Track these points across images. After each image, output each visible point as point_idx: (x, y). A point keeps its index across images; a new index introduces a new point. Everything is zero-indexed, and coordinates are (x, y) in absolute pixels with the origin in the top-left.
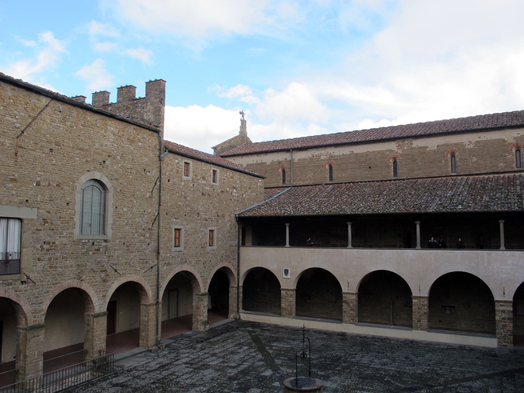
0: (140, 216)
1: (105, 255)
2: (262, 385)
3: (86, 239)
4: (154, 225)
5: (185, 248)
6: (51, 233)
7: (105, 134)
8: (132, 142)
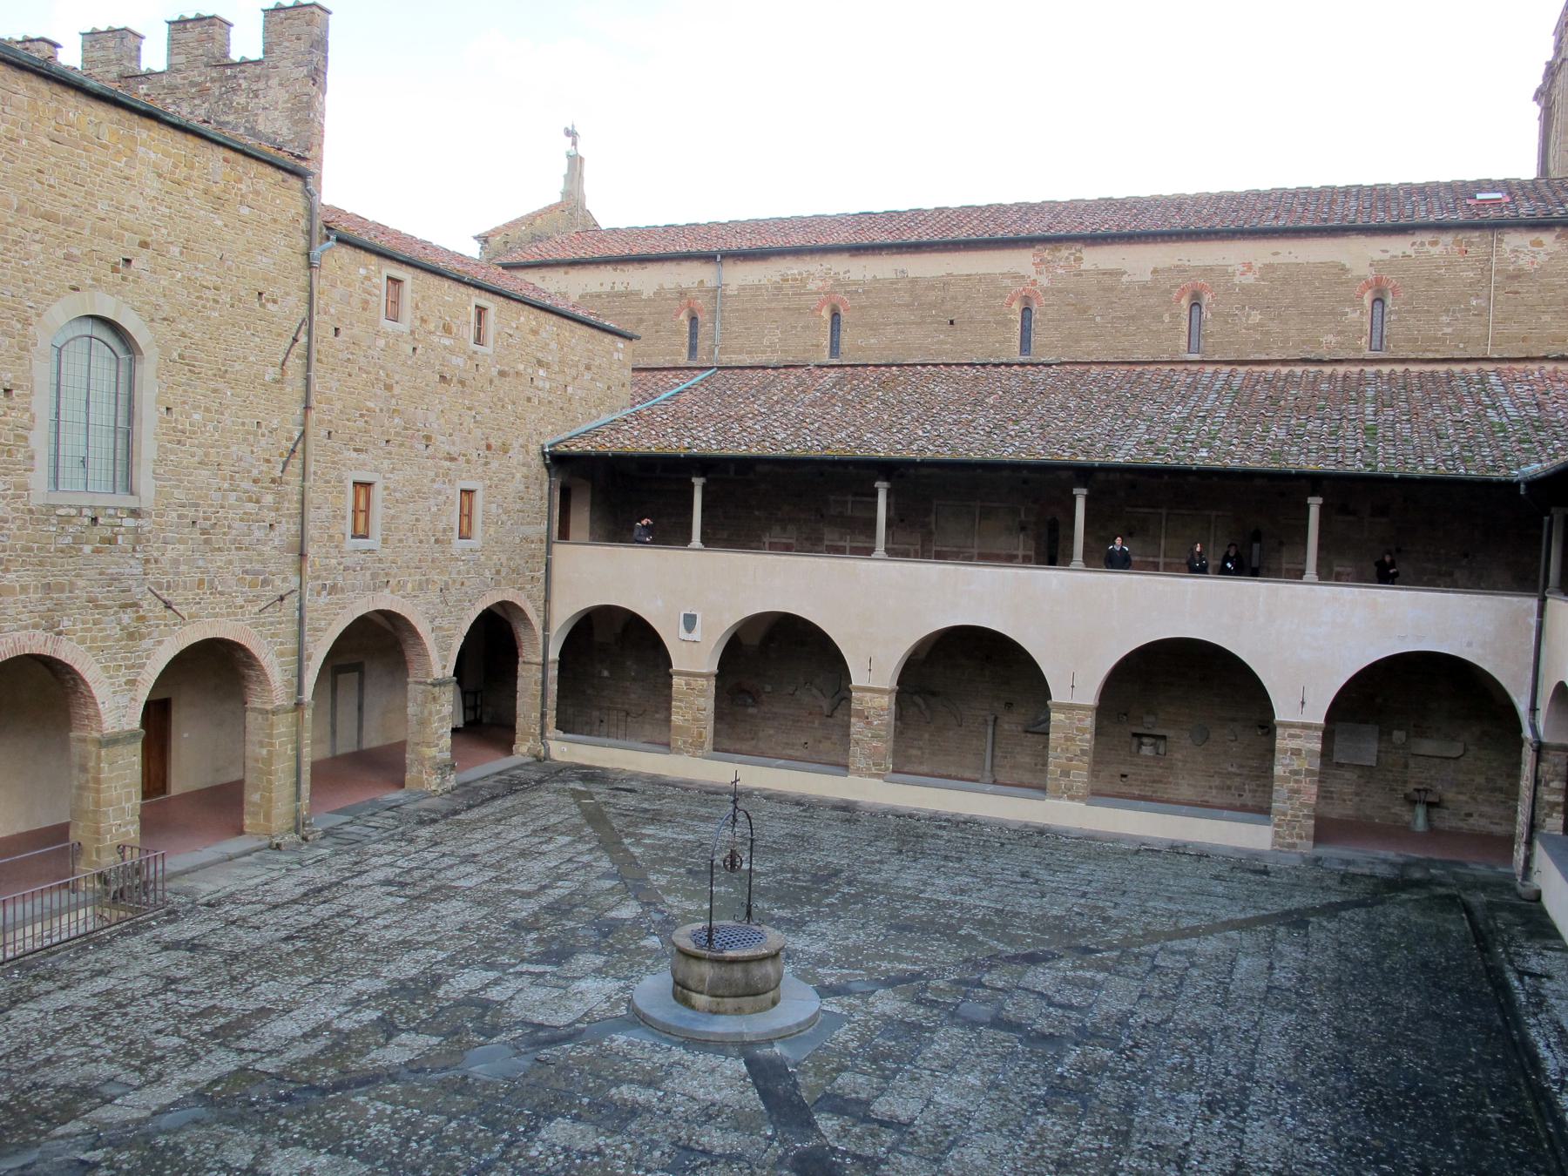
0: (245, 440)
1: (133, 557)
2: (611, 946)
3: (70, 506)
4: (289, 468)
5: (385, 541)
7: (127, 172)
8: (218, 203)
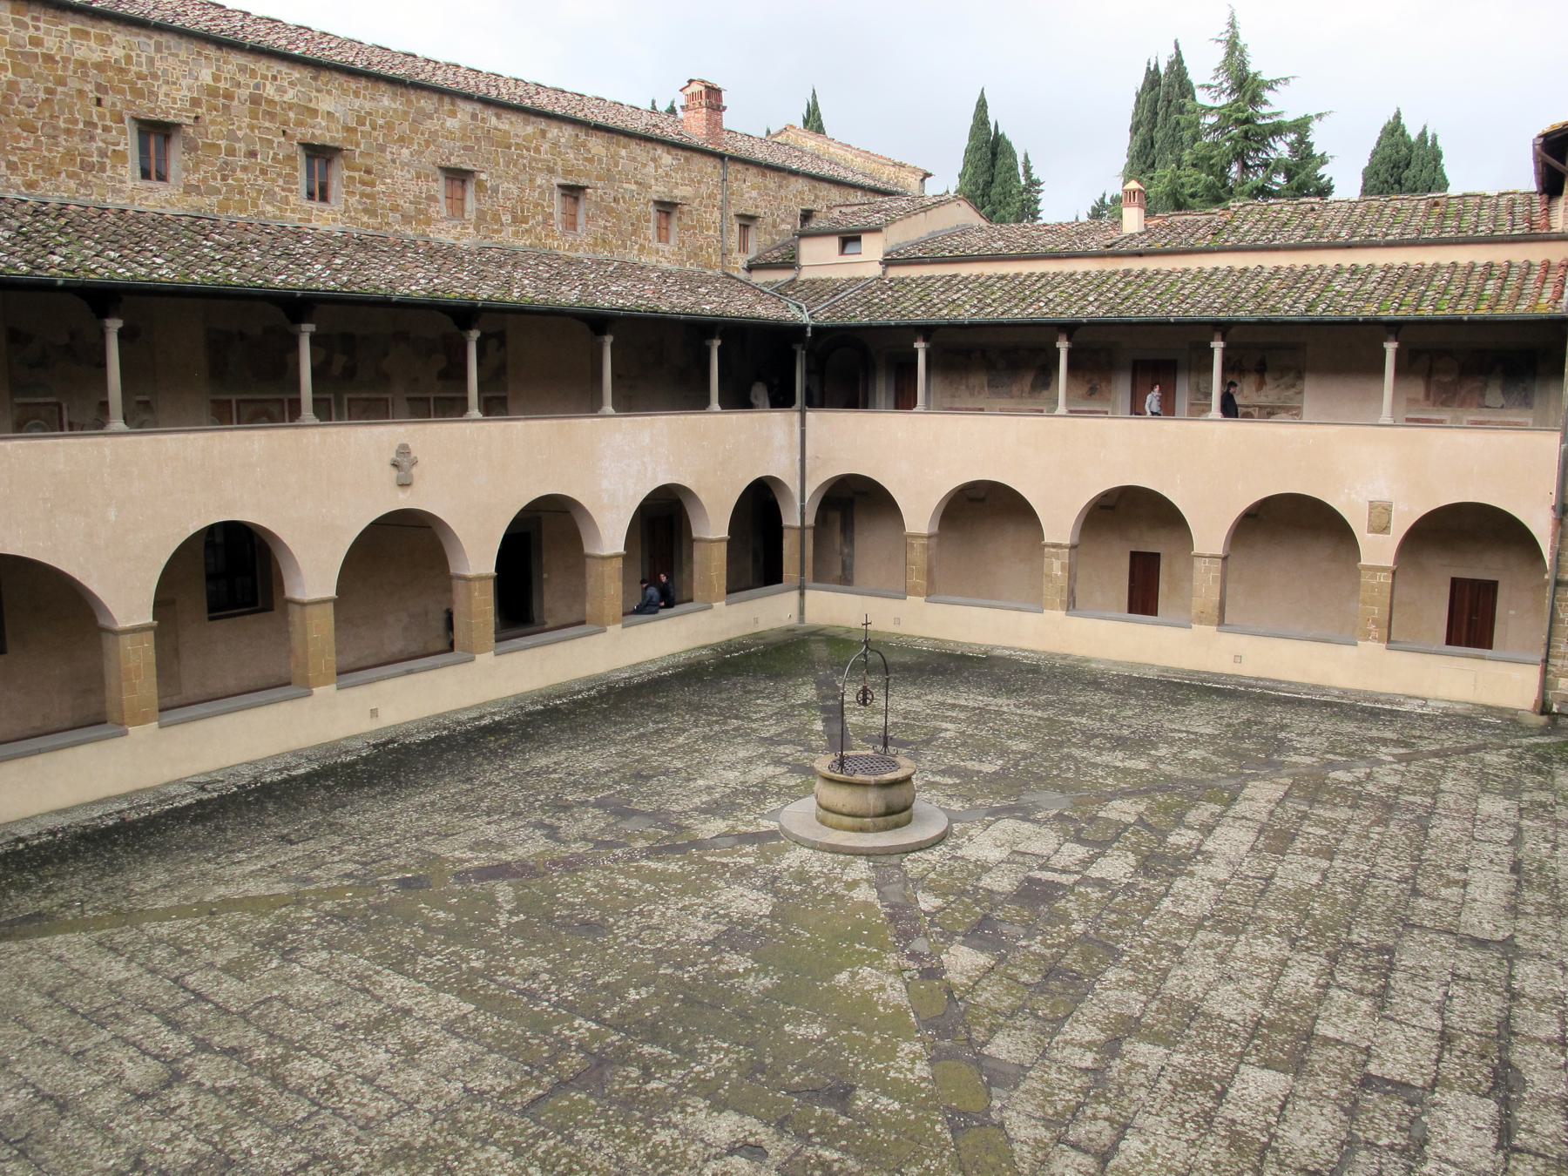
2: (977, 902)
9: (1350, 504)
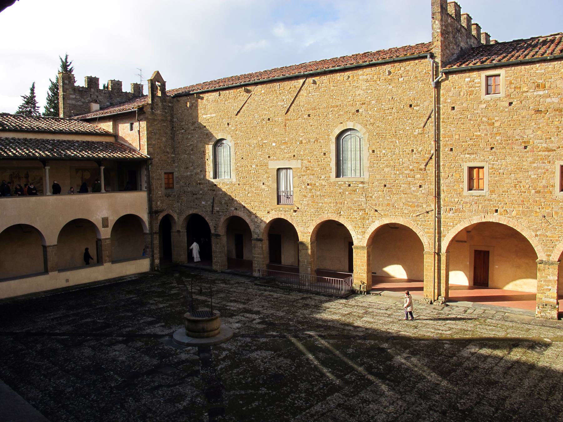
5: (492, 192)
6: (312, 177)
9: (96, 218)
